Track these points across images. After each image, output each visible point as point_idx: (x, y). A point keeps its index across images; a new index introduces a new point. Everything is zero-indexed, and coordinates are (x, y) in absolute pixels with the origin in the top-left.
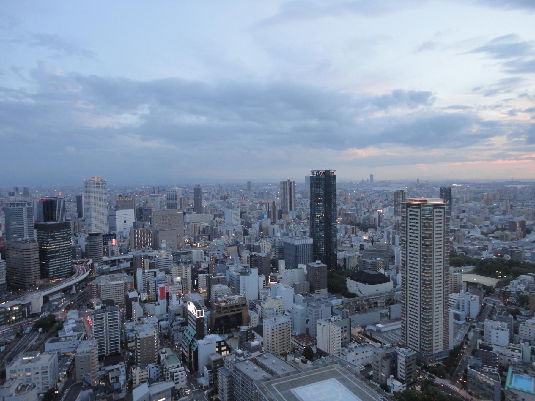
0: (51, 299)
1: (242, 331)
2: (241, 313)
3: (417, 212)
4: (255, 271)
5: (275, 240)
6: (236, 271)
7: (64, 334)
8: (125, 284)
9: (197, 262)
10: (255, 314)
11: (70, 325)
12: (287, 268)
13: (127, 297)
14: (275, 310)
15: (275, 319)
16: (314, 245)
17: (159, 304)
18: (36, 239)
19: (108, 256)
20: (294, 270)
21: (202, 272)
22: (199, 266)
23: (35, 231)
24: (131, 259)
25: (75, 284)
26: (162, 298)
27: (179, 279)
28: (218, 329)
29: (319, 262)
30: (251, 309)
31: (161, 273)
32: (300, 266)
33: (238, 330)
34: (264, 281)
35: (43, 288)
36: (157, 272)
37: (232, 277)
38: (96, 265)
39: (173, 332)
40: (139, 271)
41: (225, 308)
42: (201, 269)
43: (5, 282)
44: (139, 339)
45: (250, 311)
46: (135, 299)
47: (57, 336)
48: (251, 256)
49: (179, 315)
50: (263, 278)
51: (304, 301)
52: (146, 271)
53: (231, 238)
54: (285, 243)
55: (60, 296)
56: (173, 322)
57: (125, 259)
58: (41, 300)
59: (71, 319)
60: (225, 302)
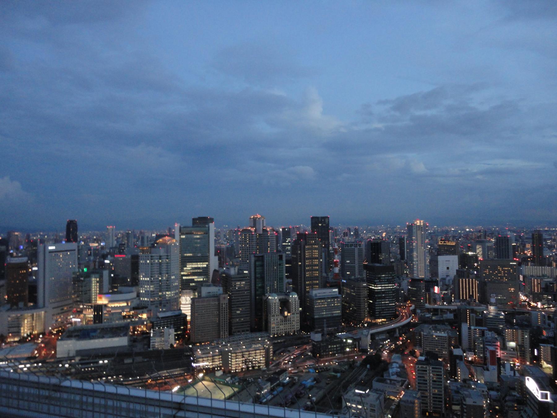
0: (377, 338)
7: (389, 376)
8: (450, 338)
9: (539, 327)
11: (394, 368)
13: (451, 352)
17: (488, 370)
18: (365, 278)
19: (430, 303)
21: (546, 341)
22: (542, 334)
23: (365, 271)
24: (454, 311)
25: (398, 327)
26: (493, 364)
27: (513, 344)
31: (490, 333)
35: (372, 325)
36: (485, 331)
38: (418, 311)
39: (506, 408)
40: (465, 327)
42: (543, 337)
43: (340, 314)
44: (465, 405)
46: (461, 358)
47: (383, 376)
49: (514, 389)
52: (472, 328)
55: (384, 337)
56: (506, 396)
57: (447, 309)
58: (369, 337)
59: (395, 362)
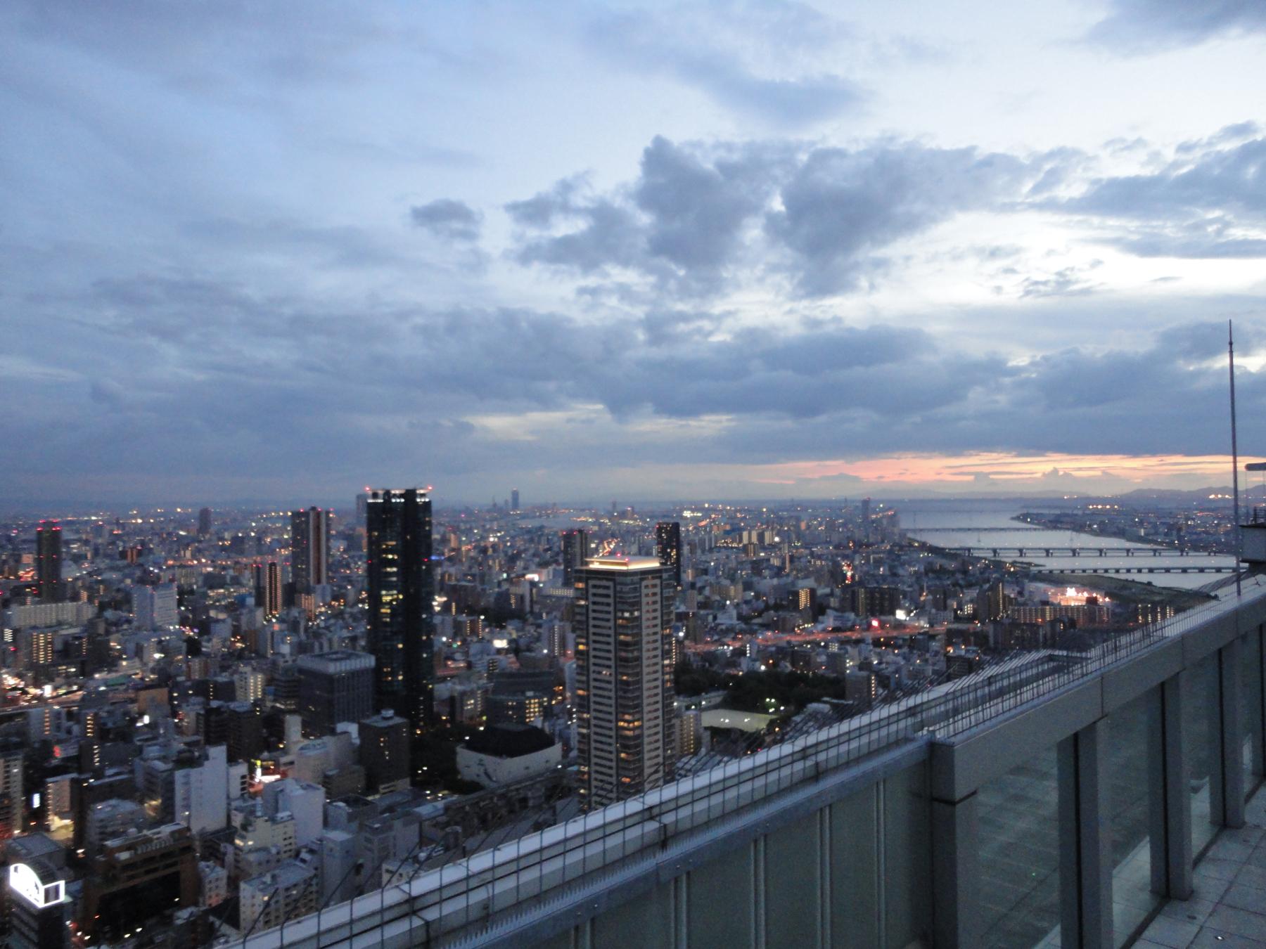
1: (179, 922)
2: (177, 874)
3: (607, 588)
4: (218, 753)
5: (274, 663)
6: (164, 759)
10: (219, 869)
12: (305, 736)
14: (274, 851)
15: (274, 877)
16: (377, 670)
20: (326, 739)
22: (50, 754)
28: (107, 928)
29: (390, 713)
30: (204, 858)
32: (341, 727)
33: (168, 921)
34: (243, 777)
37: (151, 774)
41: (128, 866)
42: (54, 762)
45: (203, 864)
48: (209, 712)
50: (242, 769)
51: (351, 818)
53: (151, 665)
54: (301, 671)
60: (128, 848)
